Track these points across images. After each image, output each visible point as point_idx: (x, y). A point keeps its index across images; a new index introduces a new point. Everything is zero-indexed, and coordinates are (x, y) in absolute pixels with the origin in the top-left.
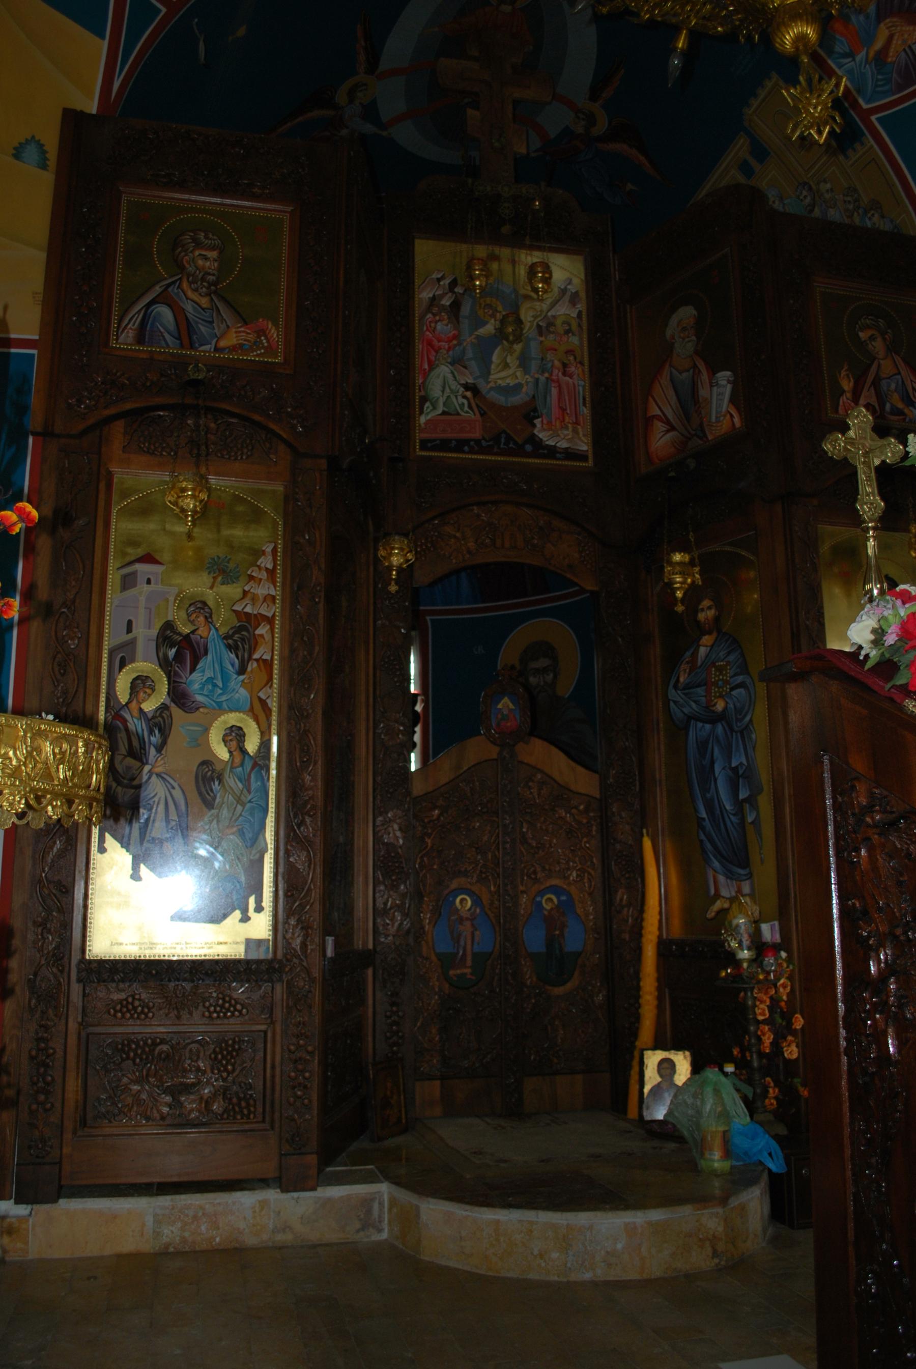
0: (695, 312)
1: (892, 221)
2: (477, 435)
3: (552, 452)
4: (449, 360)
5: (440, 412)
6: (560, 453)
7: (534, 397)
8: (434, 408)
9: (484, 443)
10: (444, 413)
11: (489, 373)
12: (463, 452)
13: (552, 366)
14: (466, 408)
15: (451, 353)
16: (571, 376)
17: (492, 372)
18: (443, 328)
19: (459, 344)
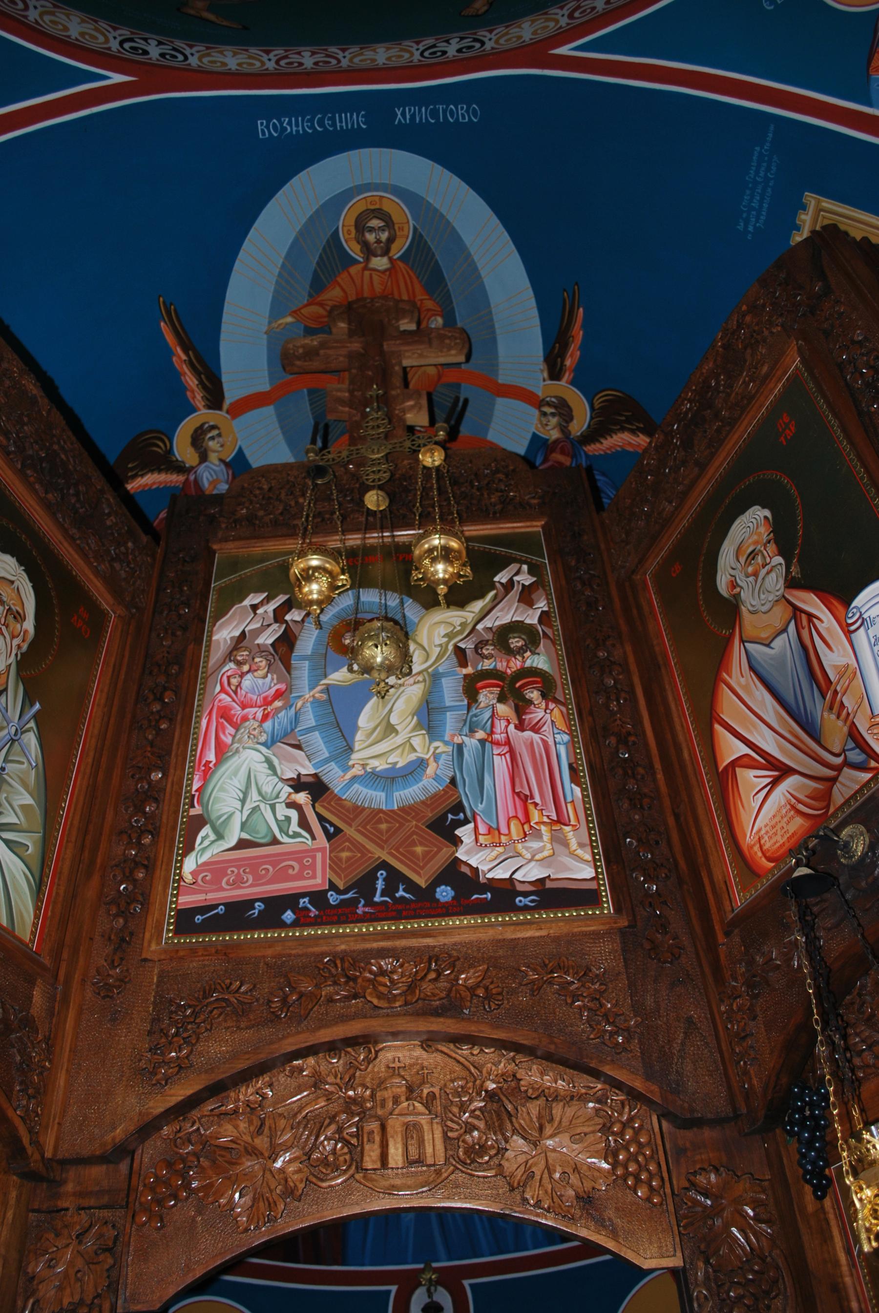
0: (767, 513)
2: (317, 882)
3: (504, 895)
4: (263, 739)
5: (233, 842)
6: (525, 894)
7: (453, 781)
8: (220, 836)
9: (333, 898)
10: (242, 844)
11: (350, 749)
12: (283, 925)
13: (493, 716)
14: (294, 827)
15: (268, 725)
16: (536, 729)
17: (357, 746)
18: (257, 683)
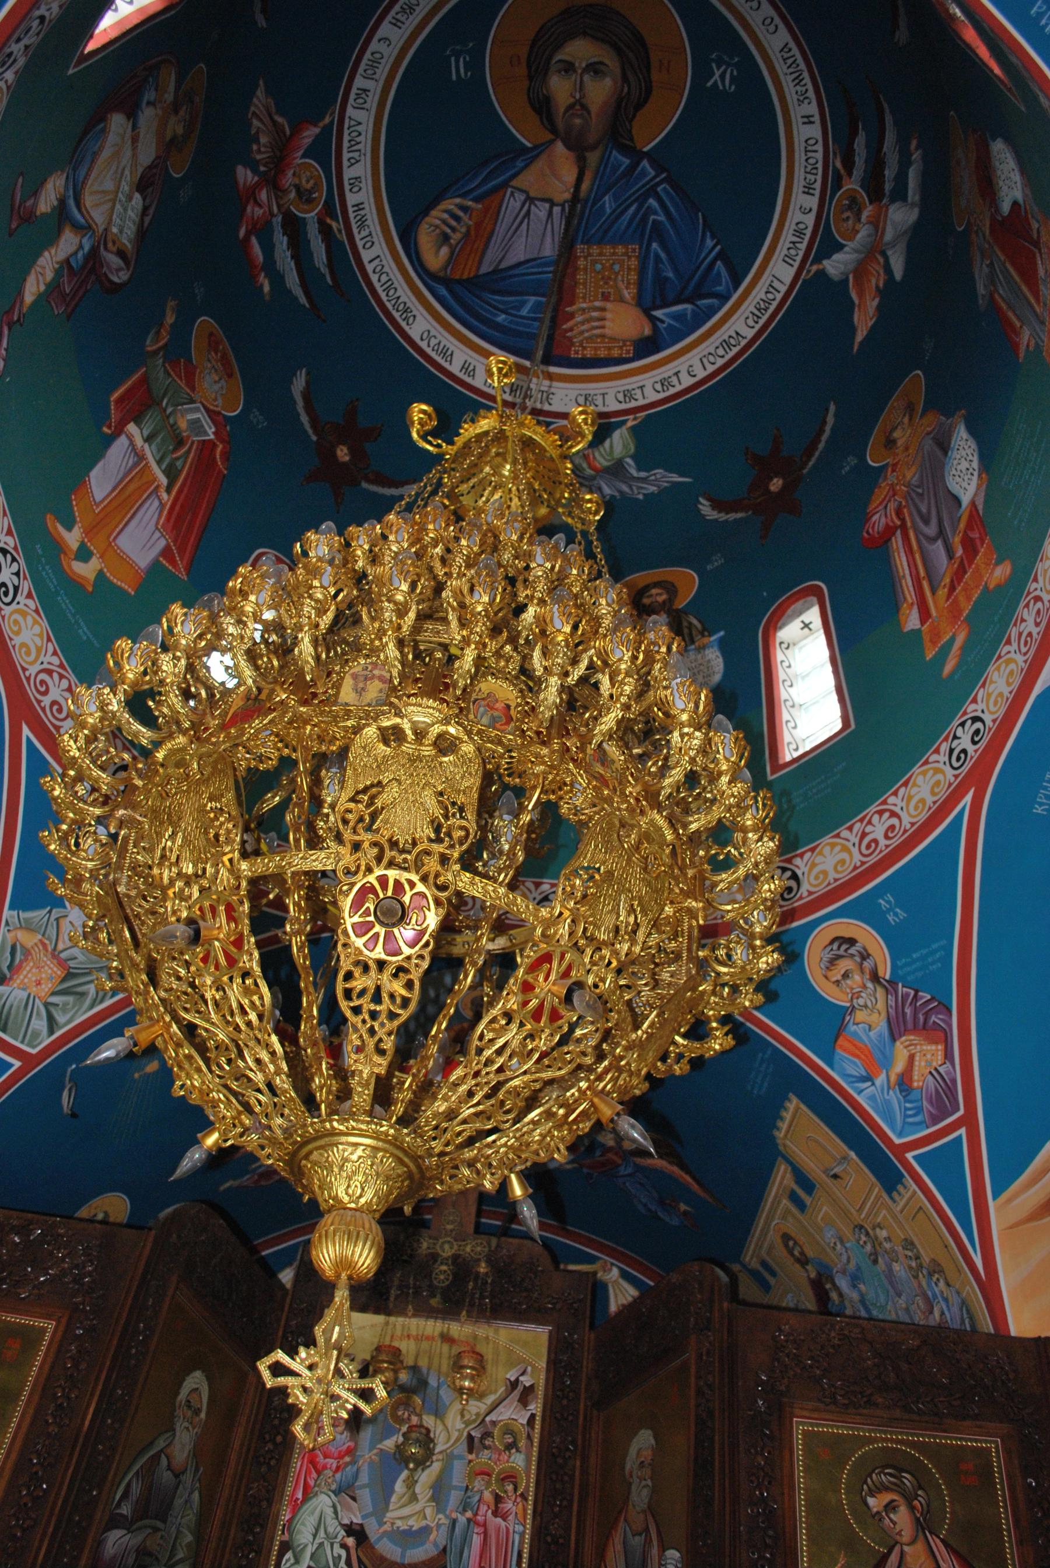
1: (958, 1293)
4: (334, 1487)
7: (444, 1550)
11: (386, 1509)
15: (338, 1476)
17: (391, 1507)
19: (353, 1462)
